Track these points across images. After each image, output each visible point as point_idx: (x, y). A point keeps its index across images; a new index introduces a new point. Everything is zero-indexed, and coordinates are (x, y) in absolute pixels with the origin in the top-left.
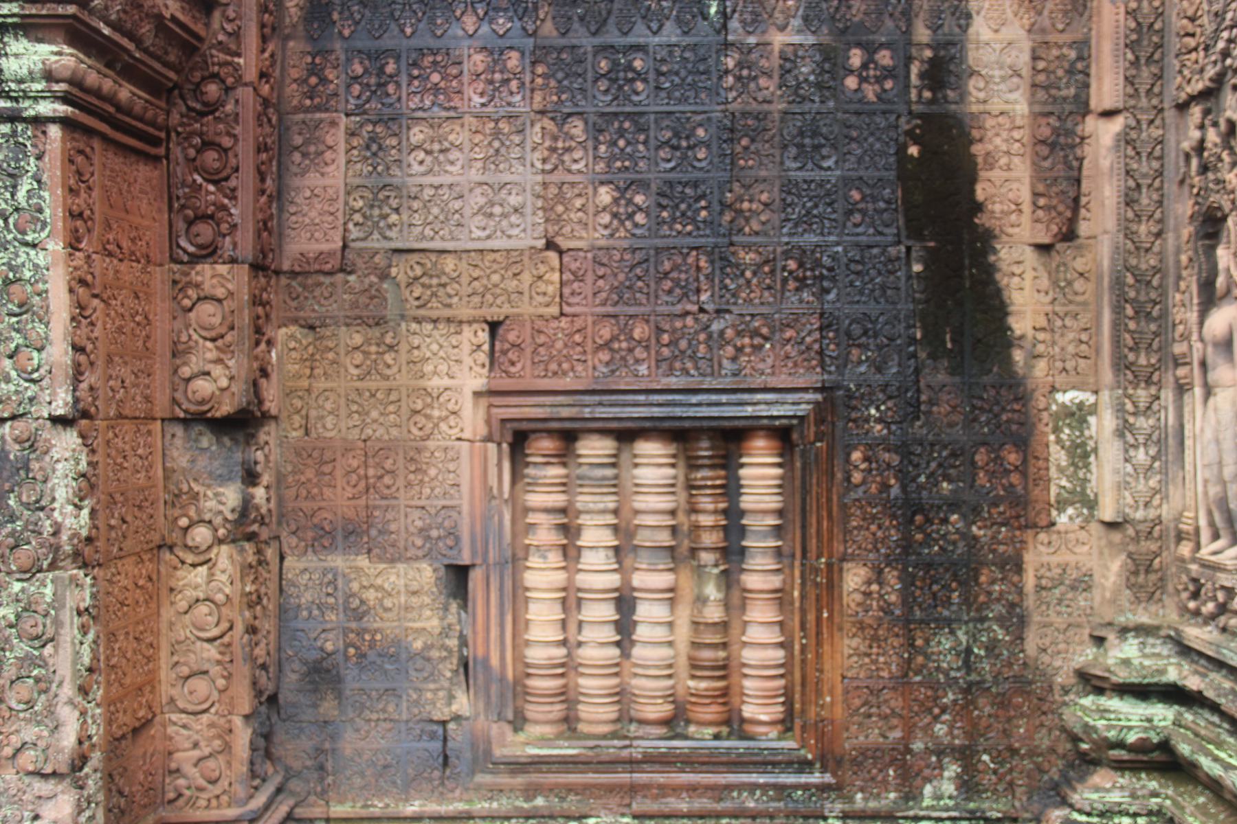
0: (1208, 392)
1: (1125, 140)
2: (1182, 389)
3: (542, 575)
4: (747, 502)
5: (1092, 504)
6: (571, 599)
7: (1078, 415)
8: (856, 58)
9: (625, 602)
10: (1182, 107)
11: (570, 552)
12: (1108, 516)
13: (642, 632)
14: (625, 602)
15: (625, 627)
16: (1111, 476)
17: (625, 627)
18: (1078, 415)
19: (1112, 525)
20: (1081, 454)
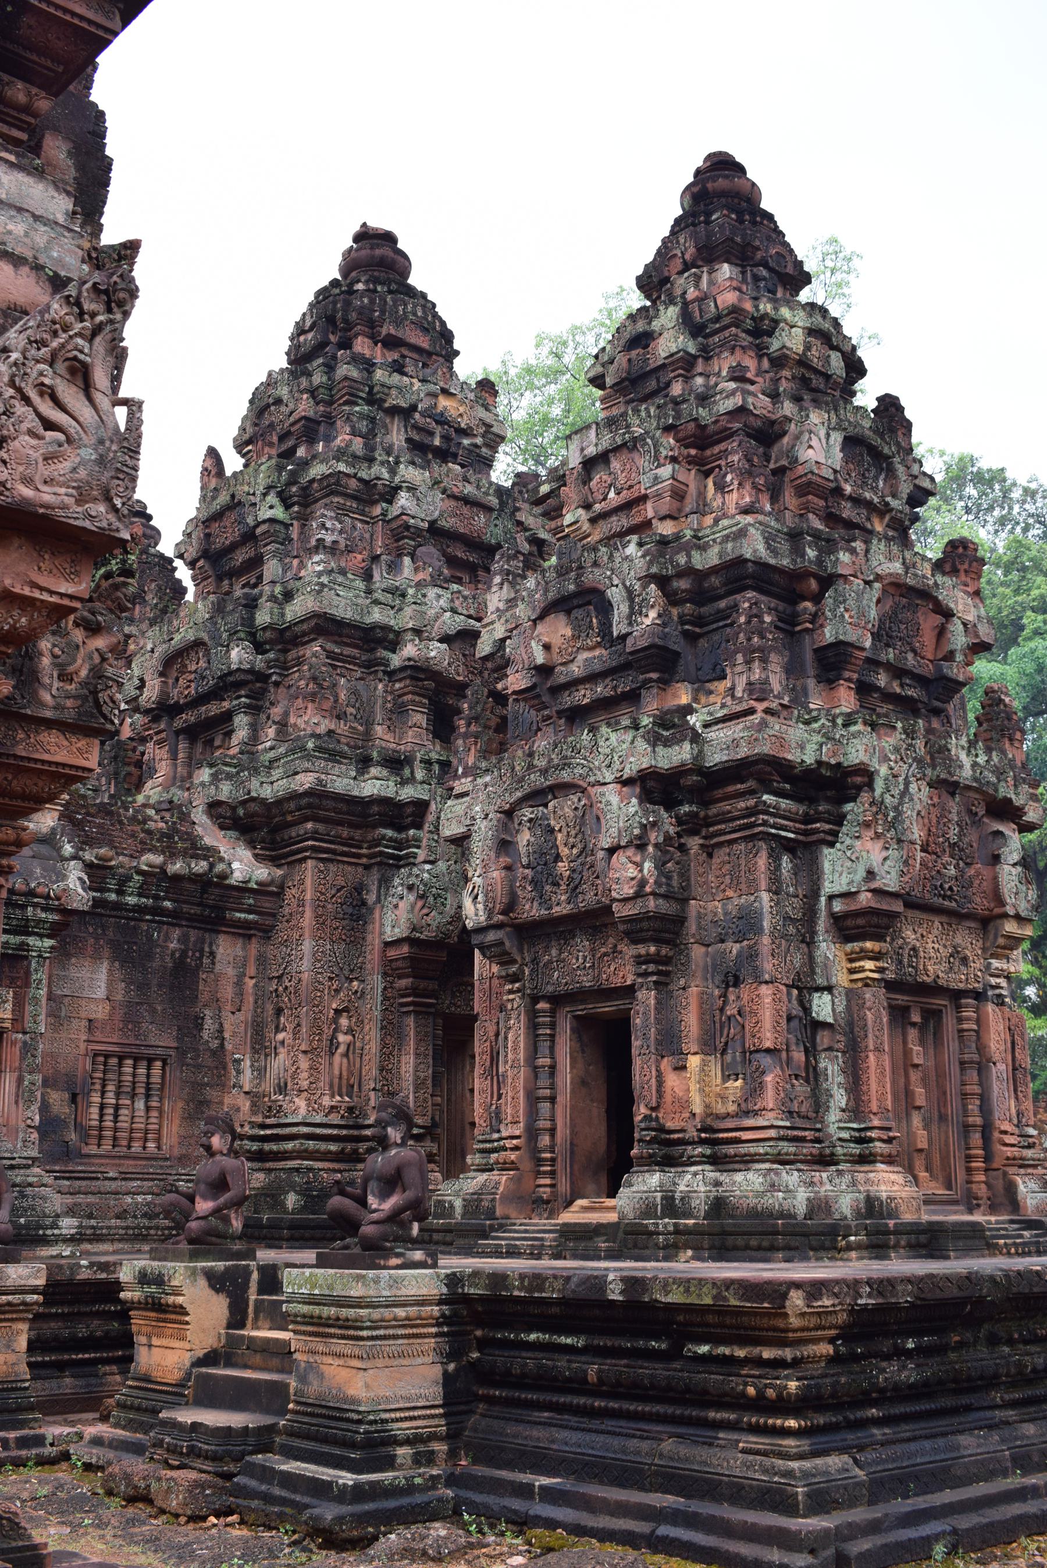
0: (276, 1054)
1: (255, 985)
2: (266, 1055)
3: (96, 1098)
4: (153, 1080)
5: (241, 1087)
6: (102, 1107)
7: (238, 1061)
8: (190, 953)
9: (117, 1108)
10: (271, 979)
11: (103, 1093)
12: (247, 1089)
13: (120, 1118)
14: (117, 1108)
15: (116, 1116)
16: (247, 1079)
17: (116, 1116)
18: (238, 1061)
19: (246, 1093)
20: (239, 1072)
